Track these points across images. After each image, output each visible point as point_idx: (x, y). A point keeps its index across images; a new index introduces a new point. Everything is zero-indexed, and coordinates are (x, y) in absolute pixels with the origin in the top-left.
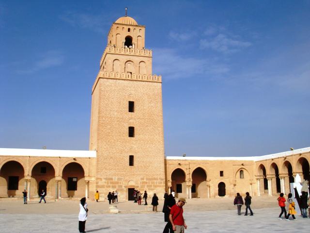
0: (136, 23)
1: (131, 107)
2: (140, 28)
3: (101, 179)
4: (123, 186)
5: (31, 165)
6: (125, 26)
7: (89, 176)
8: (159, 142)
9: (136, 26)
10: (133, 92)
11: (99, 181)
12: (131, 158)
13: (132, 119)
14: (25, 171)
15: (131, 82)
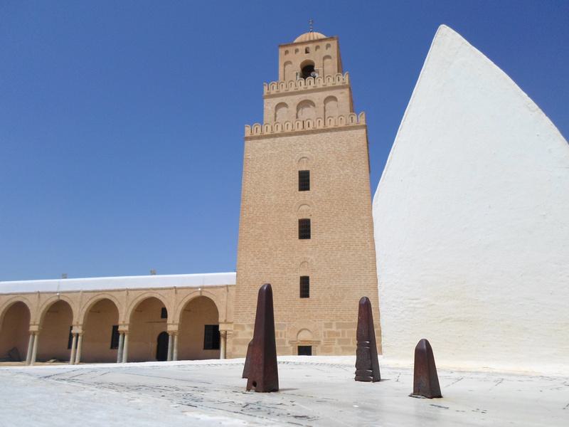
0: (321, 36)
1: (304, 181)
2: (326, 43)
3: (243, 327)
4: (287, 342)
5: (129, 304)
6: (299, 47)
7: (226, 322)
8: (364, 244)
9: (321, 40)
10: (306, 154)
11: (239, 331)
12: (305, 282)
13: (308, 204)
14: (120, 315)
15: (303, 137)
